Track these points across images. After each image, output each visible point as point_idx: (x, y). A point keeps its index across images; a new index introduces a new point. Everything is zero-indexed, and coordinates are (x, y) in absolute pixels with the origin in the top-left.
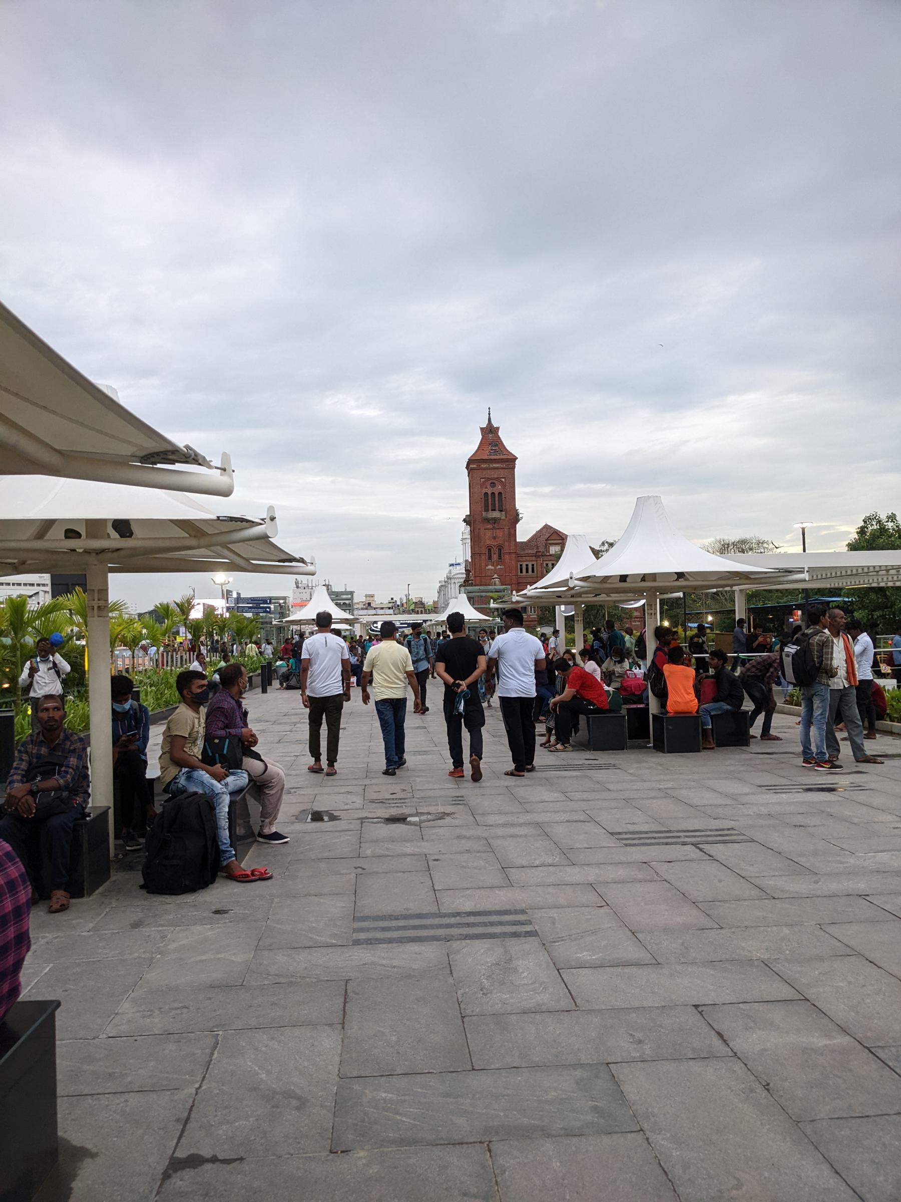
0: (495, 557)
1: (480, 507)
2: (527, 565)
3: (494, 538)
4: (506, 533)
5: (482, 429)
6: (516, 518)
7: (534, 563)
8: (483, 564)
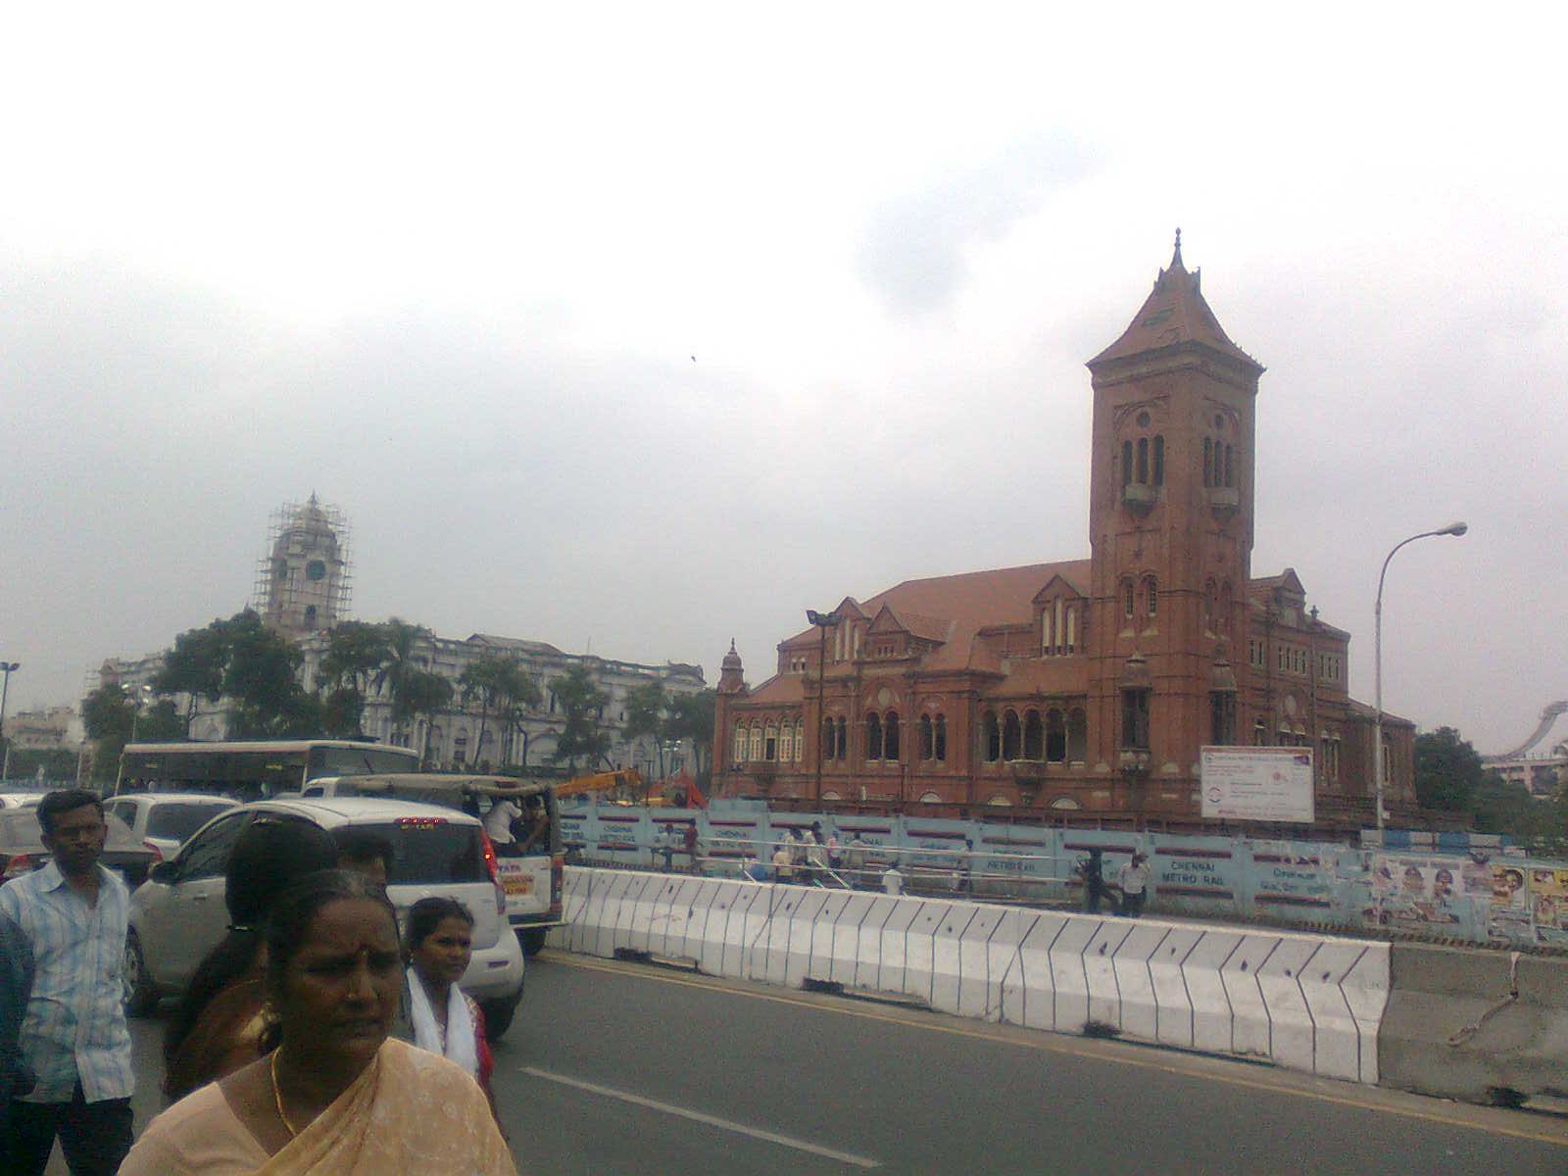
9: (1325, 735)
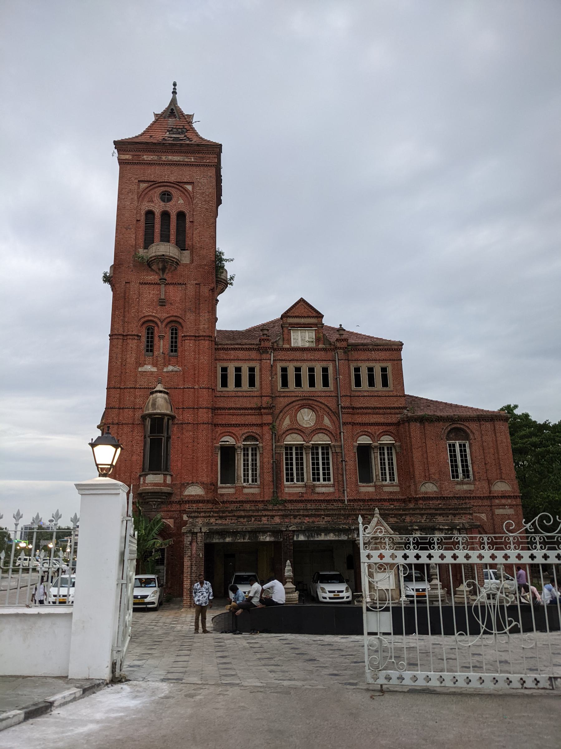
0: (162, 346)
1: (136, 236)
3: (162, 303)
4: (191, 290)
5: (156, 115)
6: (216, 277)
8: (131, 359)
9: (364, 440)
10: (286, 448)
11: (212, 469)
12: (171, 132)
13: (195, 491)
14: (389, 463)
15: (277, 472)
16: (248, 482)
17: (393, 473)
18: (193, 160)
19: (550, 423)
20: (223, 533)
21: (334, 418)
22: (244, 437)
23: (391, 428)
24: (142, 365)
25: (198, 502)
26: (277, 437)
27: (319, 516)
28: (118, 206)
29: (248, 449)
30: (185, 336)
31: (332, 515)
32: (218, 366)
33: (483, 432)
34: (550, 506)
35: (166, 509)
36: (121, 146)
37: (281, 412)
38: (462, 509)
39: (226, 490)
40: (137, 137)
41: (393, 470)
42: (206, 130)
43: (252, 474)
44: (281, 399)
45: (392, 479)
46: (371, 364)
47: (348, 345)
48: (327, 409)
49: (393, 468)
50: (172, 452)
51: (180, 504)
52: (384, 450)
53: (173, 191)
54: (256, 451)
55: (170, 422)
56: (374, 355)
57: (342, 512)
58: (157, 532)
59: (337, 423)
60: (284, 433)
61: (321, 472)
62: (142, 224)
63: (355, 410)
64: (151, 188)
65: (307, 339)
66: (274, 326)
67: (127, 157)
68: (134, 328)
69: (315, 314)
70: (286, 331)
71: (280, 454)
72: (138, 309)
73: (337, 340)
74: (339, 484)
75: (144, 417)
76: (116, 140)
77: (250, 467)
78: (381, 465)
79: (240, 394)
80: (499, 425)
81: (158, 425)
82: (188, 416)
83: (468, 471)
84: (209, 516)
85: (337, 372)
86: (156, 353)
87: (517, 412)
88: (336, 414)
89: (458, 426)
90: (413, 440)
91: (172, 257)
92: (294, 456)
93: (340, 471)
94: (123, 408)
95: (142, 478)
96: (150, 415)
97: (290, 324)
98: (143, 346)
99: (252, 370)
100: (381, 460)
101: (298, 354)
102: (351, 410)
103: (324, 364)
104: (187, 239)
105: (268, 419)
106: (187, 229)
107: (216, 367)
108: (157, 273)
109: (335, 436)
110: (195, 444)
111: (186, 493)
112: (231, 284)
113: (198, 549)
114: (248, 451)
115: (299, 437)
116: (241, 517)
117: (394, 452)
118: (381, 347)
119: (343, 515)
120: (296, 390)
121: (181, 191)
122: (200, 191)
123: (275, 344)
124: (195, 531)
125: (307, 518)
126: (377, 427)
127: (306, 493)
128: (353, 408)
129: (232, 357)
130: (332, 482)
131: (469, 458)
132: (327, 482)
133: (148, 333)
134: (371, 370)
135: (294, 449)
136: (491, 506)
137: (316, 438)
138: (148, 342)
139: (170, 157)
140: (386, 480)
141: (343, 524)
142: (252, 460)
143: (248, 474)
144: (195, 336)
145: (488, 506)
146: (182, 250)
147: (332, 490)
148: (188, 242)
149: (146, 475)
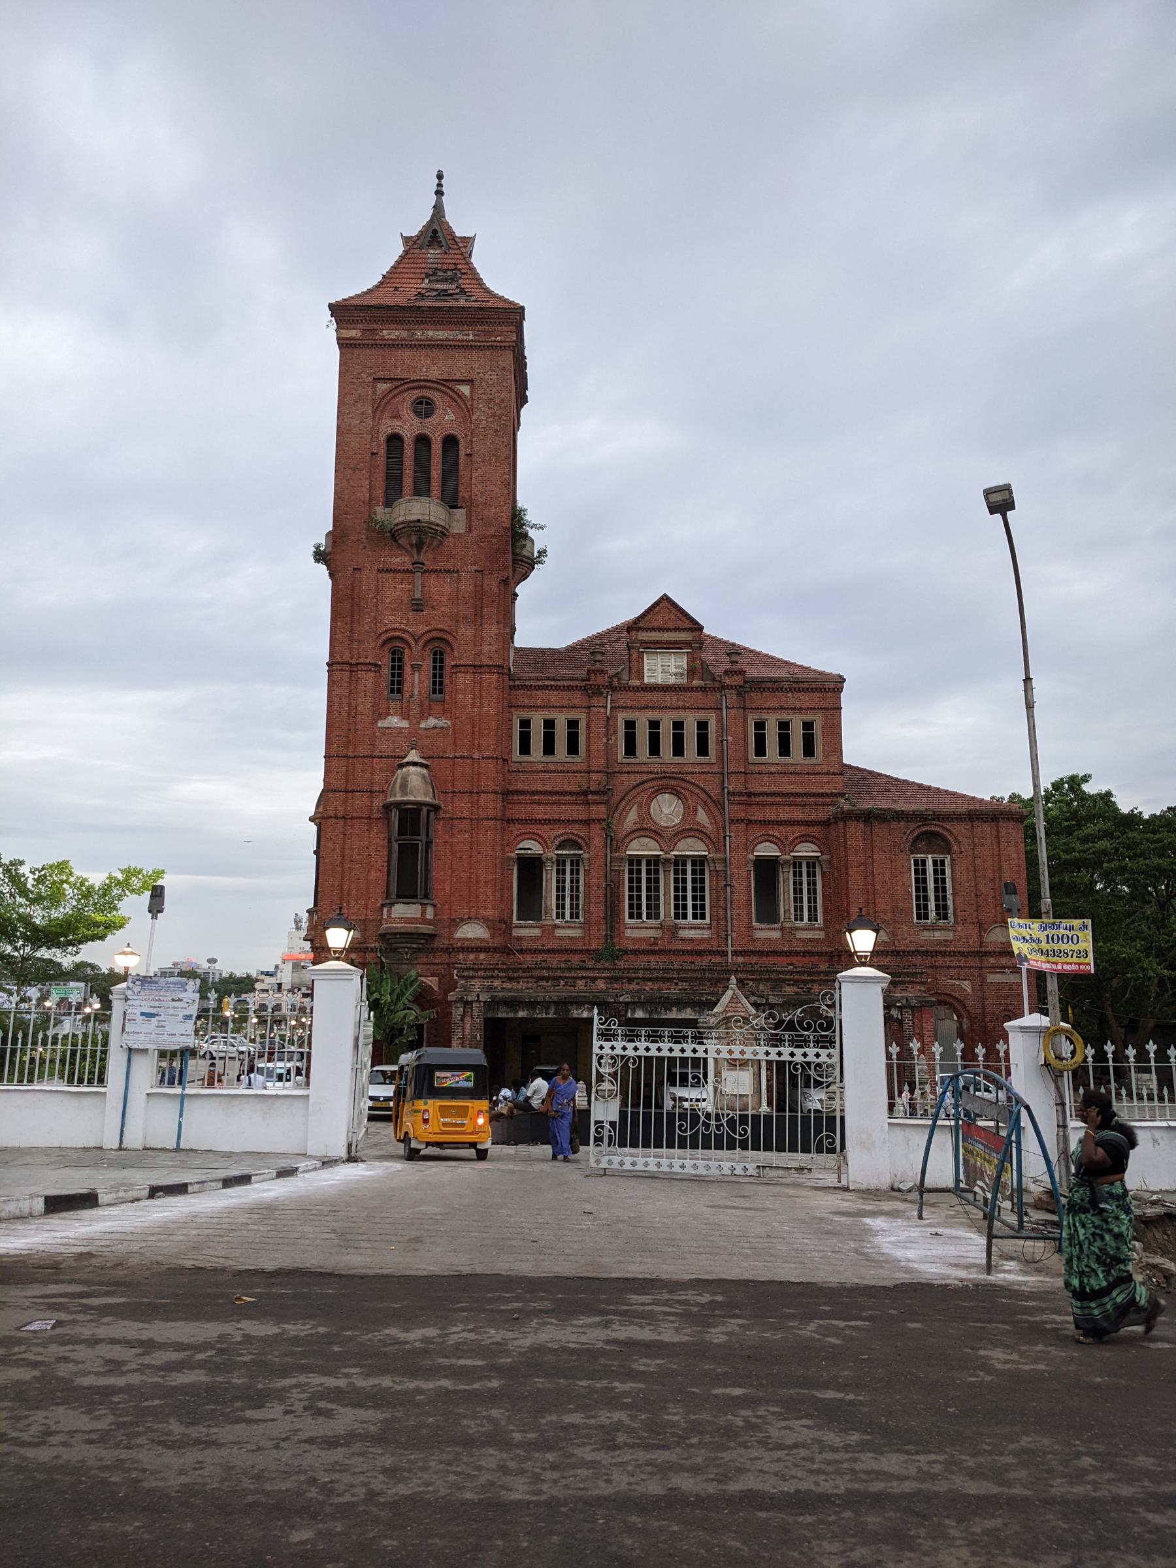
0: (417, 682)
2: (549, 724)
3: (418, 606)
4: (467, 583)
5: (406, 240)
6: (513, 553)
7: (581, 716)
8: (365, 706)
9: (767, 850)
10: (631, 863)
11: (502, 896)
12: (432, 278)
13: (472, 931)
14: (809, 890)
15: (612, 903)
16: (563, 917)
17: (815, 907)
18: (471, 337)
19: (1141, 813)
20: (513, 1003)
21: (715, 811)
22: (557, 843)
23: (814, 830)
24: (384, 716)
25: (479, 950)
26: (614, 843)
27: (670, 980)
28: (338, 427)
29: (564, 862)
30: (456, 666)
31: (691, 978)
32: (514, 717)
33: (976, 840)
34: (1111, 968)
35: (425, 960)
36: (342, 312)
37: (623, 799)
38: (908, 974)
39: (527, 931)
40: (370, 291)
41: (815, 902)
42: (499, 272)
43: (571, 905)
44: (624, 777)
45: (813, 917)
46: (784, 716)
47: (745, 682)
48: (703, 796)
49: (815, 899)
50: (435, 865)
51: (449, 953)
52: (801, 867)
53: (436, 396)
54: (578, 865)
55: (432, 815)
56: (791, 699)
57: (707, 975)
58: (410, 998)
59: (719, 819)
60: (626, 836)
61: (690, 903)
62: (381, 460)
63: (753, 798)
64: (396, 391)
65: (673, 670)
66: (619, 639)
67: (353, 333)
68: (370, 652)
69: (688, 625)
70: (635, 655)
71: (620, 873)
72: (375, 618)
73: (726, 672)
74: (720, 924)
75: (387, 807)
76: (333, 301)
77: (567, 892)
78: (795, 893)
79: (552, 767)
80: (1007, 828)
81: (411, 820)
82: (462, 806)
83: (945, 907)
84: (492, 977)
85: (722, 729)
86: (407, 695)
87: (1089, 788)
88: (719, 804)
89: (933, 829)
90: (850, 852)
91: (433, 523)
92: (644, 876)
93: (722, 903)
94: (353, 791)
95: (385, 910)
96: (397, 805)
97: (643, 642)
98: (385, 683)
99: (573, 724)
100: (795, 884)
101: (654, 697)
102: (745, 798)
103: (701, 715)
104: (461, 488)
105: (599, 811)
106: (461, 468)
107: (510, 720)
108: (407, 551)
109: (716, 843)
110: (474, 853)
111: (458, 935)
112: (540, 562)
113: (473, 1026)
114: (564, 865)
115: (653, 843)
116: (543, 978)
117: (818, 870)
118: (806, 686)
119: (710, 980)
120: (649, 761)
121: (451, 397)
122: (485, 397)
123: (615, 680)
124: (470, 999)
125: (650, 983)
126: (789, 828)
127: (661, 938)
128: (749, 795)
129: (539, 702)
130: (708, 920)
131: (948, 884)
132: (699, 921)
133: (393, 660)
134: (784, 726)
135: (644, 864)
136: (981, 968)
137: (682, 844)
138: (393, 675)
139: (430, 333)
140: (802, 920)
141: (708, 994)
142: (572, 882)
143: (564, 905)
144: (475, 666)
145: (976, 968)
146: (451, 507)
147: (706, 934)
148: (463, 493)
149: (393, 904)
